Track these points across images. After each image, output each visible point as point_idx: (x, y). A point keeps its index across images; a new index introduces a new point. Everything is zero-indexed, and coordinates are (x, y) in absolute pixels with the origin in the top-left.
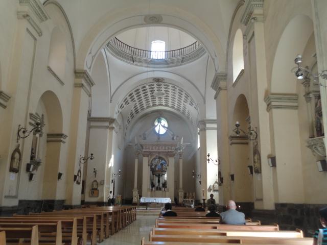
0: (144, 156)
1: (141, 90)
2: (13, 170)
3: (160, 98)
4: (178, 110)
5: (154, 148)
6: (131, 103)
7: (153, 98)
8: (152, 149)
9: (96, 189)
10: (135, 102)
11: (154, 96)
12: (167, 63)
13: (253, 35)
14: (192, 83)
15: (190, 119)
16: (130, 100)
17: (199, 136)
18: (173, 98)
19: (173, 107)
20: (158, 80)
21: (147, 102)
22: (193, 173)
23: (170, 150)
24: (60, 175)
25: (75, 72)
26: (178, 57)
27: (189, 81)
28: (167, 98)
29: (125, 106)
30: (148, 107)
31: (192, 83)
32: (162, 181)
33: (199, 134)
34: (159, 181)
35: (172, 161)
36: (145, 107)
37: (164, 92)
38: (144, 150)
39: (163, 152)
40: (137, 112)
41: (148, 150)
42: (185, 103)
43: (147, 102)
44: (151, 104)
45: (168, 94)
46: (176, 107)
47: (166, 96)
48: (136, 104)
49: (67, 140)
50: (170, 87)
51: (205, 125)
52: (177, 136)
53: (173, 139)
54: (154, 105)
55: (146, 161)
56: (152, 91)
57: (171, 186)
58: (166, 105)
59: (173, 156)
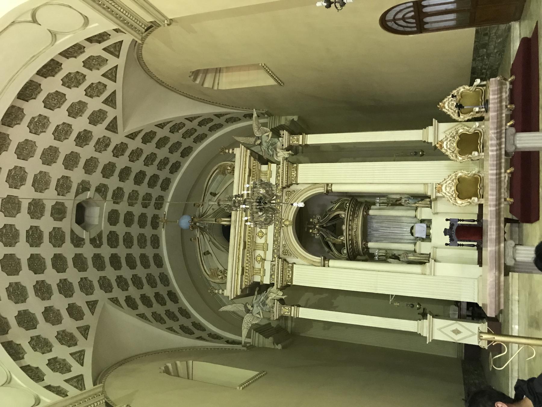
41: (267, 266)
48: (115, 301)
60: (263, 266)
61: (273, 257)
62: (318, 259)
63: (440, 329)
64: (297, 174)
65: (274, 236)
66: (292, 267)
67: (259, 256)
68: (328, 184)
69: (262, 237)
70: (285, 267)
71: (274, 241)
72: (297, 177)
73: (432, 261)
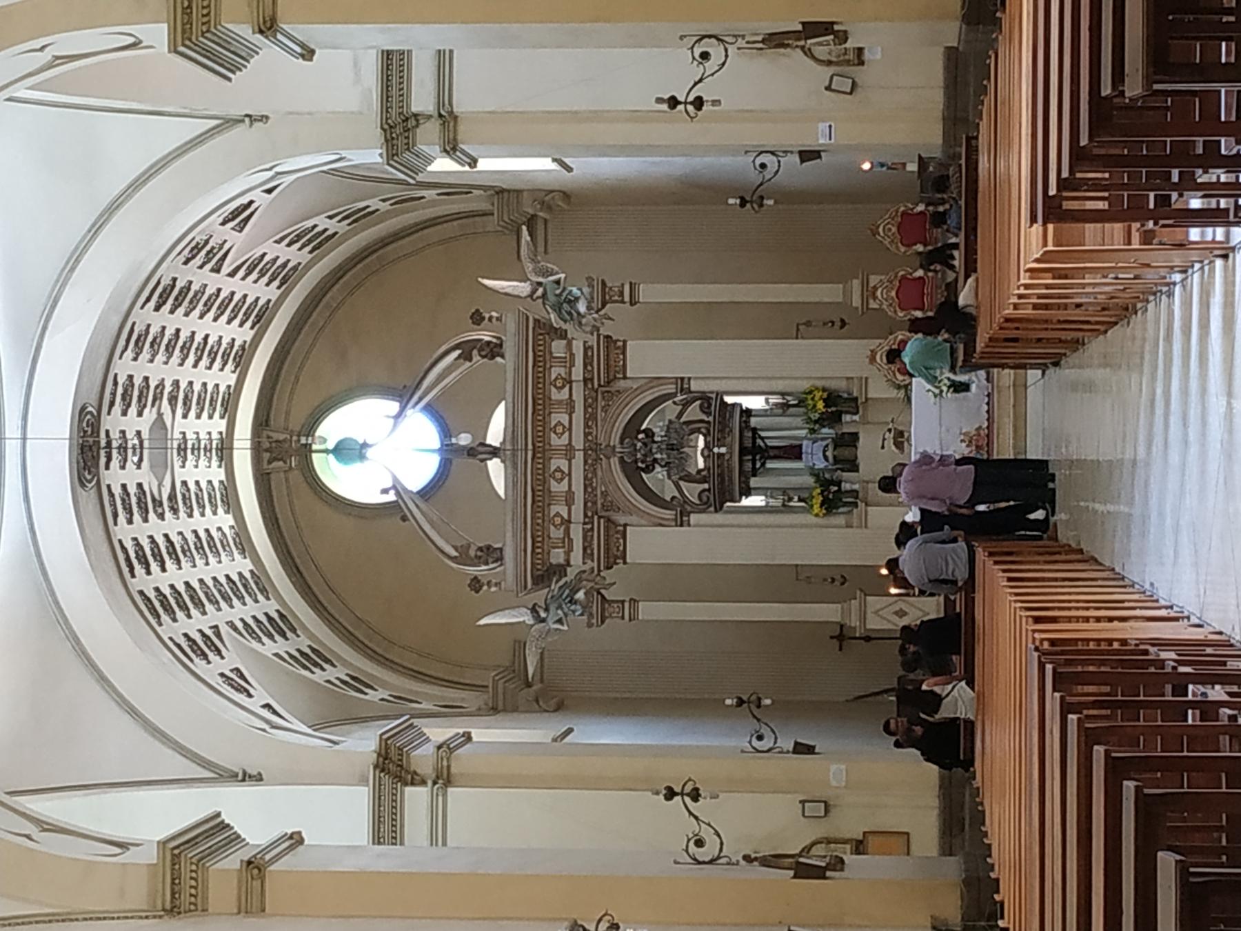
0: (614, 555)
1: (143, 582)
3: (182, 450)
4: (262, 317)
5: (564, 486)
6: (231, 660)
8: (569, 500)
10: (224, 630)
11: (172, 497)
13: (739, 111)
14: (113, 207)
15: (332, 226)
17: (484, 164)
18: (185, 349)
19: (243, 358)
20: (90, 451)
21: (206, 545)
22: (743, 202)
23: (578, 373)
25: (173, 910)
27: (96, 229)
29: (261, 696)
30: (243, 543)
31: (113, 207)
32: (794, 429)
33: (473, 162)
34: (794, 452)
35: (650, 359)
37: (150, 414)
38: (577, 556)
39: (590, 419)
40: (281, 625)
41: (577, 533)
42: (226, 269)
43: (206, 545)
44: (226, 521)
45: (161, 385)
46: (244, 334)
47: (173, 400)
50: (124, 367)
51: (416, 115)
52: (477, 318)
53: (493, 350)
54: (230, 498)
55: (651, 543)
56: (143, 504)
57: (838, 361)
58: (229, 405)
59: (614, 348)
60: (567, 532)
61: (586, 516)
62: (668, 514)
63: (876, 612)
64: (624, 360)
65: (586, 478)
66: (624, 533)
67: (558, 515)
68: (682, 379)
69: (562, 479)
70: (611, 533)
71: (585, 487)
72: (624, 366)
73: (861, 505)
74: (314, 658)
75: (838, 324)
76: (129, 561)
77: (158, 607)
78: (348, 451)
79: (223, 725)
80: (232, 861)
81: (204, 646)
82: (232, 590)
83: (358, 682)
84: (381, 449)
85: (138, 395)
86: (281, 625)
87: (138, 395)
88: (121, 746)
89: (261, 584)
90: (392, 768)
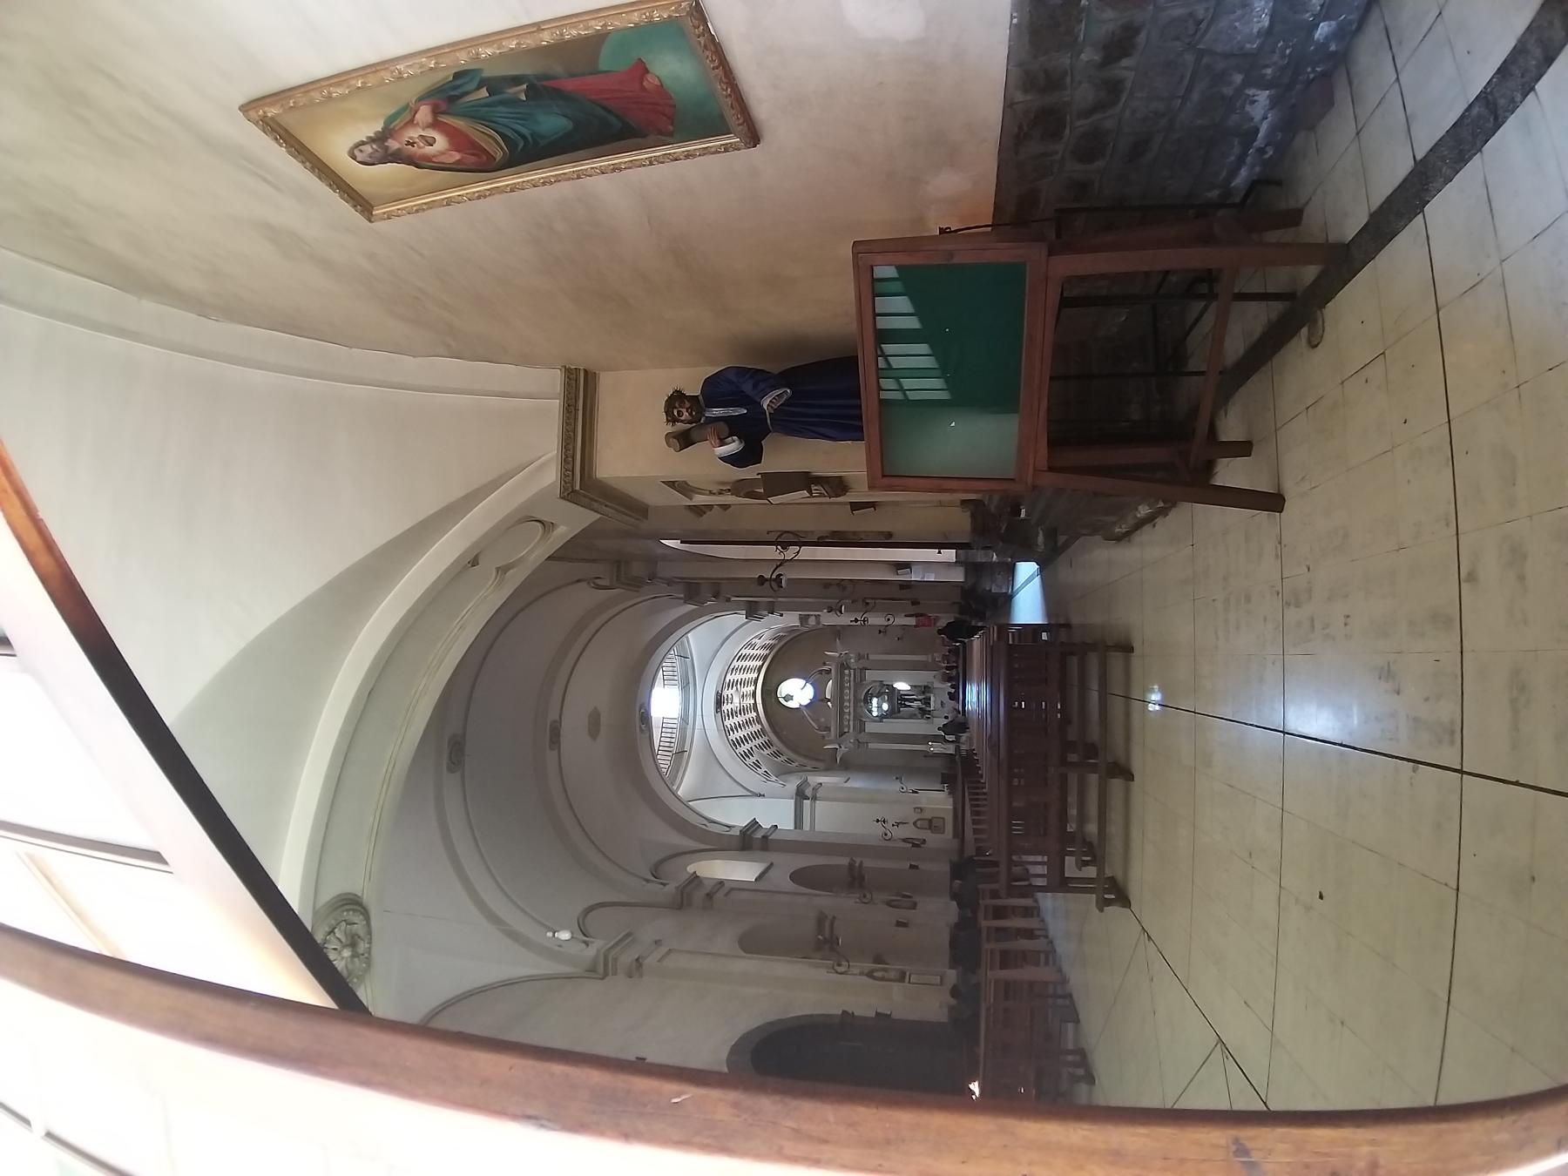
0: (862, 730)
1: (732, 737)
2: (914, 906)
7: (743, 711)
9: (930, 821)
12: (686, 685)
16: (753, 759)
20: (719, 701)
24: (912, 867)
26: (678, 664)
28: (743, 683)
30: (759, 721)
36: (756, 728)
40: (768, 744)
43: (749, 723)
49: (858, 861)
53: (829, 672)
56: (733, 714)
57: (925, 677)
74: (777, 754)
75: (923, 667)
76: (728, 731)
77: (735, 744)
78: (789, 698)
79: (753, 780)
80: (759, 835)
81: (749, 754)
82: (756, 735)
83: (790, 761)
84: (797, 692)
85: (731, 685)
86: (768, 744)
87: (731, 685)
88: (726, 786)
89: (763, 732)
90: (800, 795)
